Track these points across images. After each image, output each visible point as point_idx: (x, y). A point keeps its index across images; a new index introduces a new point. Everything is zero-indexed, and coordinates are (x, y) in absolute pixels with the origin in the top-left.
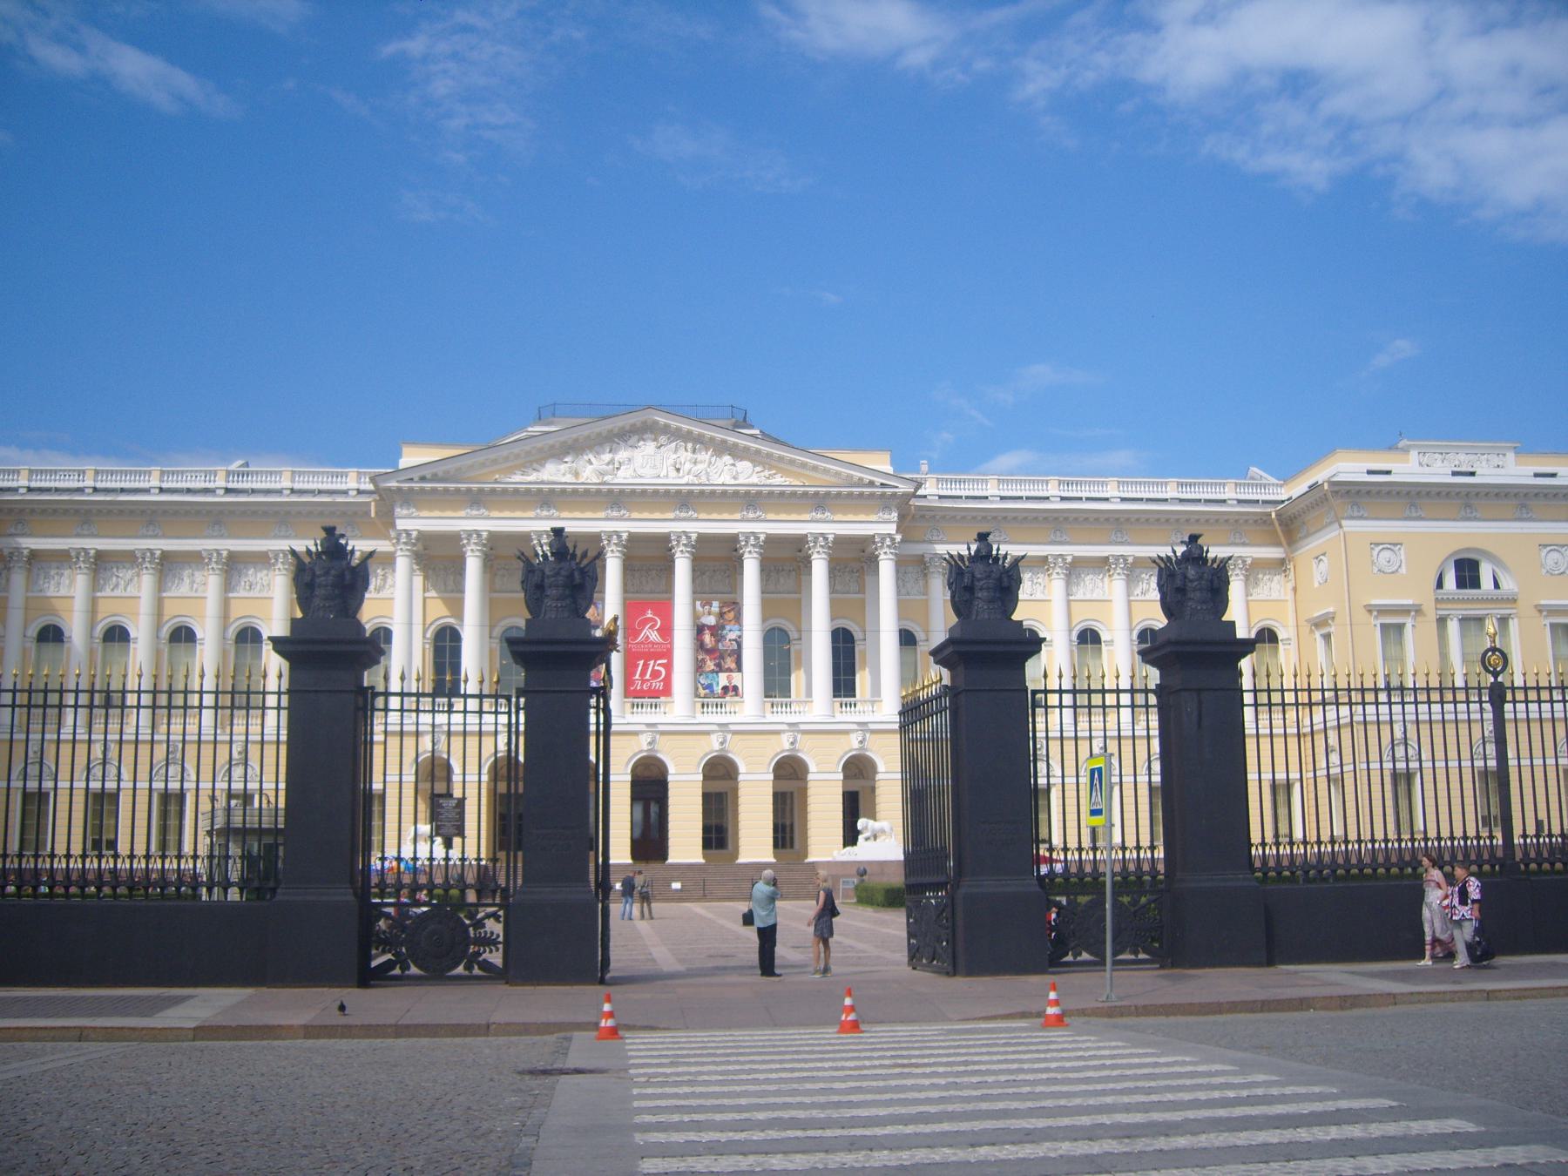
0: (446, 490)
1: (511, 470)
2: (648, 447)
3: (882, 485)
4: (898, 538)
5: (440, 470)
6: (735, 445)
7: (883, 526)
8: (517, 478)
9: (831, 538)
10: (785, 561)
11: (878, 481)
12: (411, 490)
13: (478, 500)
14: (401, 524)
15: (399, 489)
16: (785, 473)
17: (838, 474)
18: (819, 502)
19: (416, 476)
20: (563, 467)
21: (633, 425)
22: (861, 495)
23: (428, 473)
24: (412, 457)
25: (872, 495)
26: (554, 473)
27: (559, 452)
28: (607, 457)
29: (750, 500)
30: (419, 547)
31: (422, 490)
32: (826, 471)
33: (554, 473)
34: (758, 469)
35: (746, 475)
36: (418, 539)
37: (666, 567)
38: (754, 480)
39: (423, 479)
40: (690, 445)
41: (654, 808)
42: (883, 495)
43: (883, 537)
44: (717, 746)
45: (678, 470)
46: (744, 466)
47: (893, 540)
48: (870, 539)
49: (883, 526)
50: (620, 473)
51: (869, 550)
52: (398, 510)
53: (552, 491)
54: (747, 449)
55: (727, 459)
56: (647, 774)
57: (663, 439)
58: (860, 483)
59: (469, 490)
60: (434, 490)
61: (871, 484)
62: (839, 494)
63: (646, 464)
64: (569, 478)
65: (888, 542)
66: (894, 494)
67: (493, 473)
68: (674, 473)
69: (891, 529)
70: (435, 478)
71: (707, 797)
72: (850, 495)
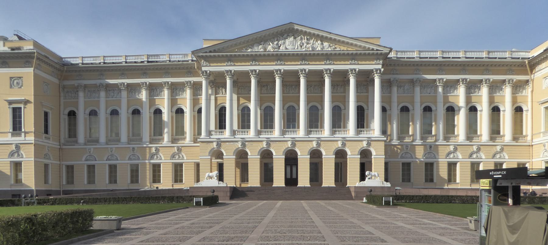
0: (219, 56)
3: (377, 50)
4: (382, 70)
5: (216, 48)
7: (376, 66)
10: (340, 81)
11: (375, 48)
12: (206, 56)
13: (230, 59)
17: (360, 46)
19: (208, 51)
22: (369, 54)
23: (212, 49)
25: (373, 54)
31: (210, 56)
36: (210, 74)
39: (210, 52)
42: (377, 54)
45: (301, 46)
46: (326, 44)
47: (380, 70)
49: (376, 66)
53: (256, 55)
54: (326, 37)
58: (369, 49)
59: (227, 56)
60: (215, 56)
61: (373, 50)
62: (361, 54)
66: (381, 54)
68: (299, 48)
69: (380, 67)
72: (365, 54)
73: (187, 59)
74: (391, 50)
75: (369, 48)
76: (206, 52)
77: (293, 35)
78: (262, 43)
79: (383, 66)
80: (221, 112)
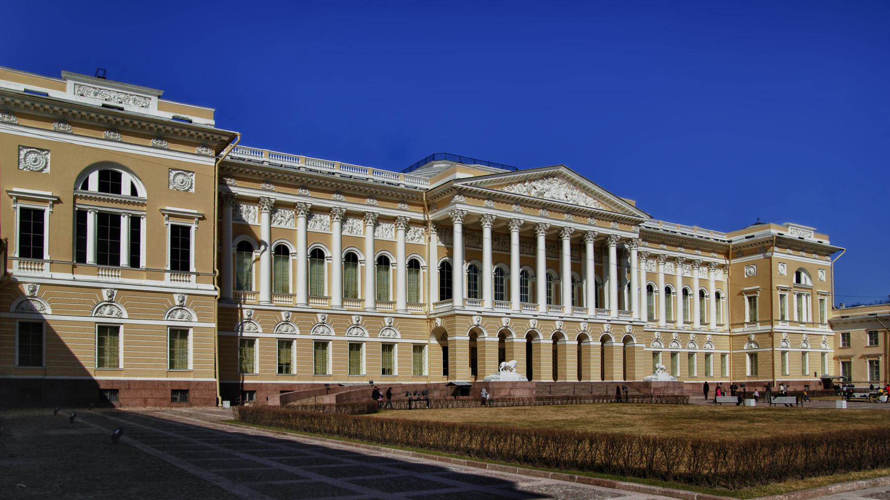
7: (632, 233)
8: (506, 189)
20: (525, 189)
26: (519, 190)
35: (591, 203)
48: (629, 240)
63: (556, 191)
69: (637, 236)
70: (475, 185)
78: (526, 184)
80: (446, 271)
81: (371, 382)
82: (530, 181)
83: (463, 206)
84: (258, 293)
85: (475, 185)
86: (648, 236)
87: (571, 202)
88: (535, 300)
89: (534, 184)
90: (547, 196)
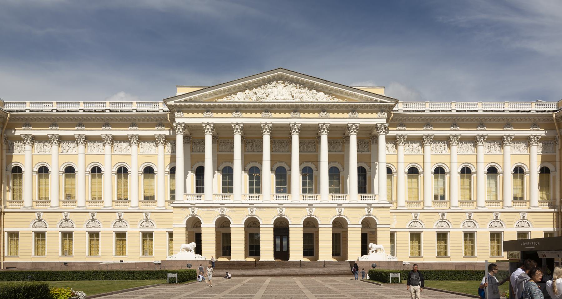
1: (222, 97)
2: (280, 86)
3: (381, 102)
4: (387, 125)
6: (317, 85)
8: (225, 99)
9: (358, 125)
10: (339, 137)
11: (379, 99)
12: (181, 106)
13: (208, 109)
14: (177, 120)
15: (176, 106)
16: (339, 97)
17: (361, 97)
18: (353, 109)
19: (182, 99)
21: (274, 77)
22: (371, 106)
24: (181, 91)
26: (239, 98)
27: (243, 89)
28: (263, 91)
29: (323, 109)
30: (187, 131)
32: (356, 96)
33: (239, 98)
34: (327, 96)
36: (185, 127)
37: (289, 142)
38: (325, 100)
39: (185, 101)
40: (298, 85)
41: (285, 242)
42: (381, 106)
43: (382, 124)
44: (309, 213)
45: (293, 96)
48: (375, 127)
50: (268, 98)
51: (375, 132)
52: (176, 114)
54: (322, 87)
55: (315, 91)
56: (281, 225)
57: (287, 83)
58: (371, 101)
61: (376, 101)
63: (280, 93)
64: (247, 100)
65: (383, 127)
66: (386, 106)
67: (215, 99)
68: (292, 98)
69: (384, 121)
71: (305, 235)
73: (157, 109)
74: (397, 102)
75: (371, 99)
76: (180, 101)
77: (284, 83)
78: (247, 91)
79: (388, 120)
81: (486, 261)
82: (251, 89)
83: (182, 119)
84: (157, 201)
85: (191, 100)
86: (399, 121)
87: (297, 100)
88: (317, 190)
89: (255, 90)
90: (269, 99)
